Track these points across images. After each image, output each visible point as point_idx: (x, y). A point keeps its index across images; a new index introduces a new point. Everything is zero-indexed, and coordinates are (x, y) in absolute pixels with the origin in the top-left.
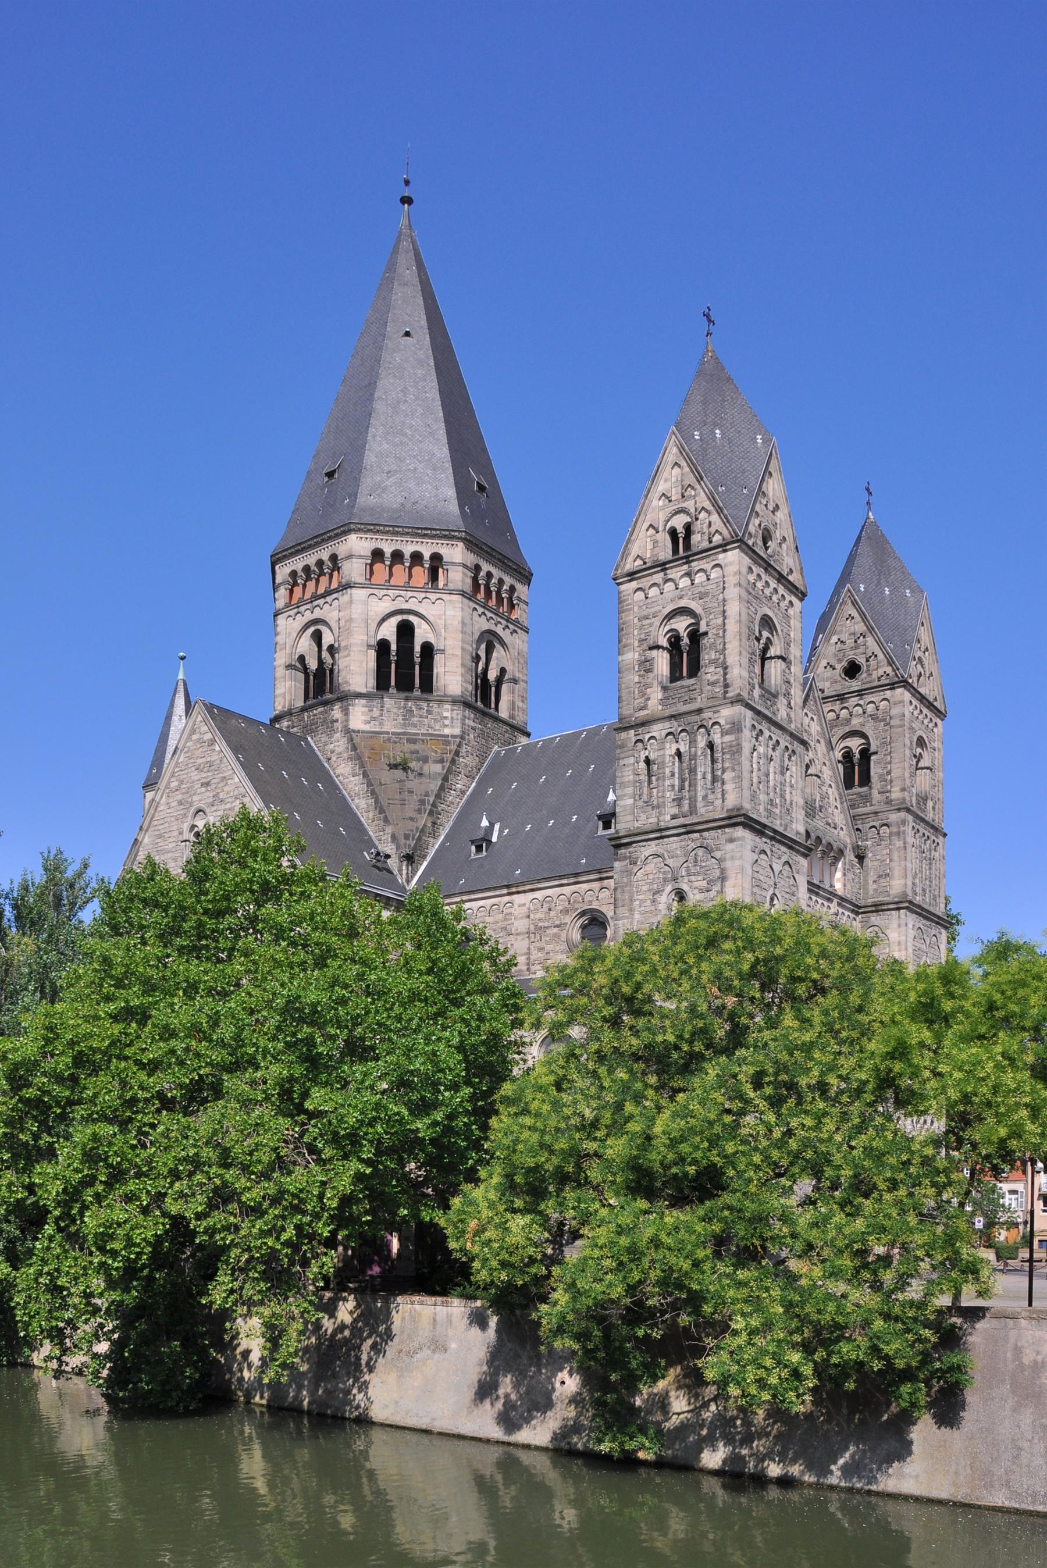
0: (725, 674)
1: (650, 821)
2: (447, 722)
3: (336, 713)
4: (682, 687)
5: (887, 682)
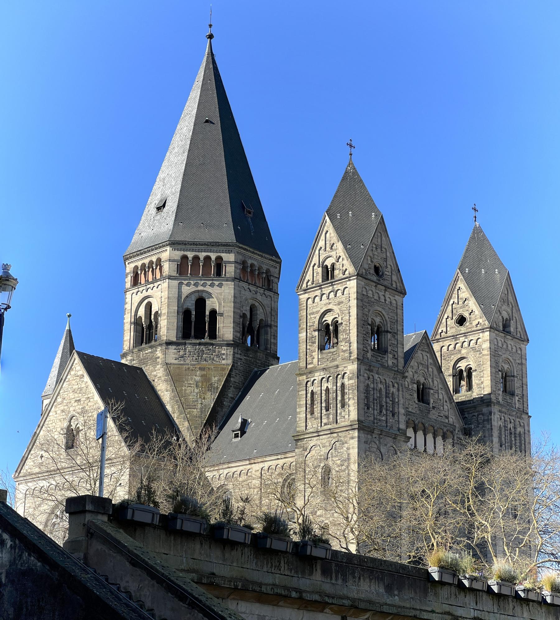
0: (350, 347)
1: (314, 426)
2: (224, 357)
3: (159, 353)
4: (330, 353)
5: (480, 328)
